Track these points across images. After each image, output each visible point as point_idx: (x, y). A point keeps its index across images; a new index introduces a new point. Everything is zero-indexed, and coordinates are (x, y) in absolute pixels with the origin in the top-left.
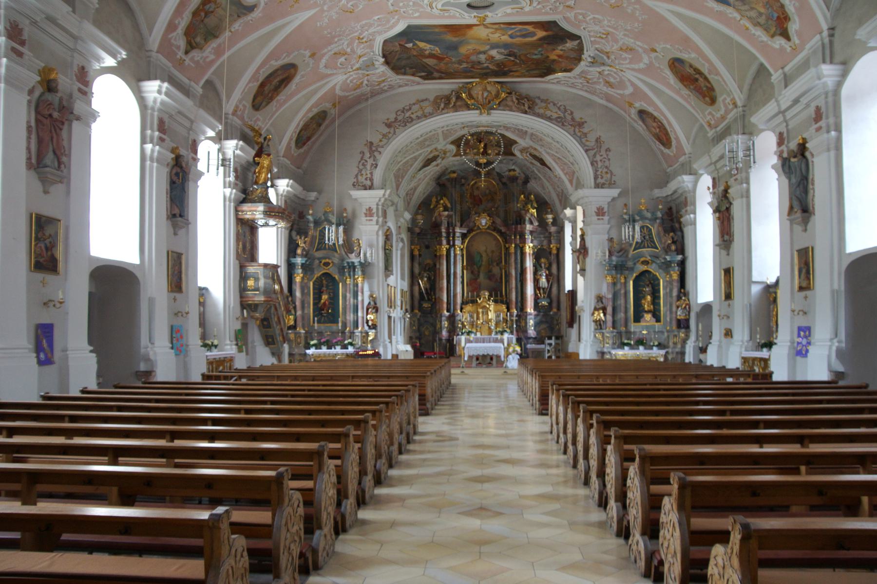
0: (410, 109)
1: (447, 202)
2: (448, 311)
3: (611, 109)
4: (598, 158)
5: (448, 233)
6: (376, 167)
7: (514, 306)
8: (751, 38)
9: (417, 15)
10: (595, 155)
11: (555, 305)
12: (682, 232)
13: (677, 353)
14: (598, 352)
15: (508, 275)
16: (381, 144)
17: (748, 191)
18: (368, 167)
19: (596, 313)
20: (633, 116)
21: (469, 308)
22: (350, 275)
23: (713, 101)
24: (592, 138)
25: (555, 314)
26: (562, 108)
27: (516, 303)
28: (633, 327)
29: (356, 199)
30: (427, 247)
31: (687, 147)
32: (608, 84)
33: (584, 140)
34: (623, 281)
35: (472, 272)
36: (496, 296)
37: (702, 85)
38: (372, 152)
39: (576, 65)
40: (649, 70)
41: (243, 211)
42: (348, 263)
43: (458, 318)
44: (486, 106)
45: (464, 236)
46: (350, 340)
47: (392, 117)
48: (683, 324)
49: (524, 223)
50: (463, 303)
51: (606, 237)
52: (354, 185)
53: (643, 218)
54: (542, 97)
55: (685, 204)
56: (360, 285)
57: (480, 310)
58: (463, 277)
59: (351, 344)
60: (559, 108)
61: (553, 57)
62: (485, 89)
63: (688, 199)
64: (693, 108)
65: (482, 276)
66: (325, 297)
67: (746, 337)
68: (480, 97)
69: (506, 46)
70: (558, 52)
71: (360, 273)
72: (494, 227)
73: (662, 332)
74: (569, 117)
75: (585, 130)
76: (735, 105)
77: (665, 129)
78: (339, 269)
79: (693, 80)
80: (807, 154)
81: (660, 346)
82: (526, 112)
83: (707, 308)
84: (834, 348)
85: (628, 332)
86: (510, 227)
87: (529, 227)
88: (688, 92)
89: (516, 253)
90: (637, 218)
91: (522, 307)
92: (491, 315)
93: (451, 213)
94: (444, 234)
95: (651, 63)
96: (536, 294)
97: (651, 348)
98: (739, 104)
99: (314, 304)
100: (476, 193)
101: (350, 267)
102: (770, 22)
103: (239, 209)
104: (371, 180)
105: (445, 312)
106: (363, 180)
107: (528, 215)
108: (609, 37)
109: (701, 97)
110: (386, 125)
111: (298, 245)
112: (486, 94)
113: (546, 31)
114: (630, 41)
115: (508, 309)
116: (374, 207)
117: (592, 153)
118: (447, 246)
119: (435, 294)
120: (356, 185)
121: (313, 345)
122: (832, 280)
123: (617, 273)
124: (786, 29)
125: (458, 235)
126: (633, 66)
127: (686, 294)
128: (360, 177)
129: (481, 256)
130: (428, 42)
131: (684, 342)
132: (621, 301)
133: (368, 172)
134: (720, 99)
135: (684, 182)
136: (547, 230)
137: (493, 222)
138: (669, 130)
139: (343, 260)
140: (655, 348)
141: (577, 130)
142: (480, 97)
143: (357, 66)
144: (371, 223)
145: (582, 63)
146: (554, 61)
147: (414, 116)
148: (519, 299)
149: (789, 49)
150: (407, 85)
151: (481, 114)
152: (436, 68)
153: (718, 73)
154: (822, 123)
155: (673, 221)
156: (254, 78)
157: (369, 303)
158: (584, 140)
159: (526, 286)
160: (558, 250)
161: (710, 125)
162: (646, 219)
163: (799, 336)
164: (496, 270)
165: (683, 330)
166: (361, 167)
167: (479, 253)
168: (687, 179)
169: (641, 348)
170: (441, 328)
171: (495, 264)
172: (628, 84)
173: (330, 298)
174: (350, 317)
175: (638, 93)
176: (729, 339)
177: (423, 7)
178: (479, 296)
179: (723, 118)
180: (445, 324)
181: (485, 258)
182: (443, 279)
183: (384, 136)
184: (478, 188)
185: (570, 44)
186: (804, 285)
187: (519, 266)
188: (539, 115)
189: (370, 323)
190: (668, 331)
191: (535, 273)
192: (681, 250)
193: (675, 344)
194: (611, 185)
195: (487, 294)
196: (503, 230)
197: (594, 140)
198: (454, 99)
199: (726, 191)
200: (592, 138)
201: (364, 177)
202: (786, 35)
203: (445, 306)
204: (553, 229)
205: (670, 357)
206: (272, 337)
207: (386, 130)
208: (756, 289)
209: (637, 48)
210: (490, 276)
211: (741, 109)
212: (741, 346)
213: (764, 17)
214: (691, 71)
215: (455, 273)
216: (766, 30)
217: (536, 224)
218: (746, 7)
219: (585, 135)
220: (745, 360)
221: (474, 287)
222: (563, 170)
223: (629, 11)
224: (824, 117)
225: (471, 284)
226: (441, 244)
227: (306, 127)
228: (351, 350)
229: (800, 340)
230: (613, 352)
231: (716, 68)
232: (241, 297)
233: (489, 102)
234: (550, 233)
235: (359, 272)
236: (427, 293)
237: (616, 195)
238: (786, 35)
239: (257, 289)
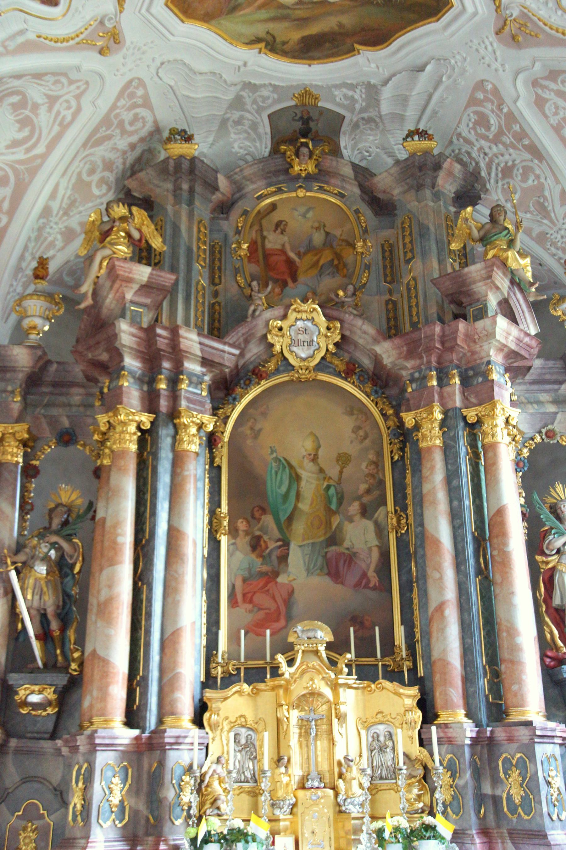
1: (149, 229)
2: (133, 718)
5: (151, 357)
7: (456, 693)
15: (413, 549)
21: (234, 704)
27: (468, 679)
30: (67, 438)
35: (256, 545)
36: (365, 647)
43: (178, 758)
45: (224, 389)
49: (482, 313)
50: (209, 682)
57: (294, 715)
58: (212, 562)
65: (297, 557)
72: (344, 358)
89: (449, 451)
91: (497, 707)
92: (349, 741)
93: (168, 278)
94: (131, 363)
100: (273, 241)
115: (428, 708)
118: (146, 419)
119: (81, 641)
125: (193, 367)
129: (296, 478)
148: (481, 660)
164: (359, 535)
171: (354, 508)
181: (310, 485)
182: (113, 561)
184: (280, 226)
187: (468, 502)
191: (535, 544)
195: (324, 634)
196: (388, 352)
203: (118, 692)
210: (335, 563)
215: (174, 536)
221: (262, 605)
225: (248, 598)
226: (112, 401)
236: (44, 636)
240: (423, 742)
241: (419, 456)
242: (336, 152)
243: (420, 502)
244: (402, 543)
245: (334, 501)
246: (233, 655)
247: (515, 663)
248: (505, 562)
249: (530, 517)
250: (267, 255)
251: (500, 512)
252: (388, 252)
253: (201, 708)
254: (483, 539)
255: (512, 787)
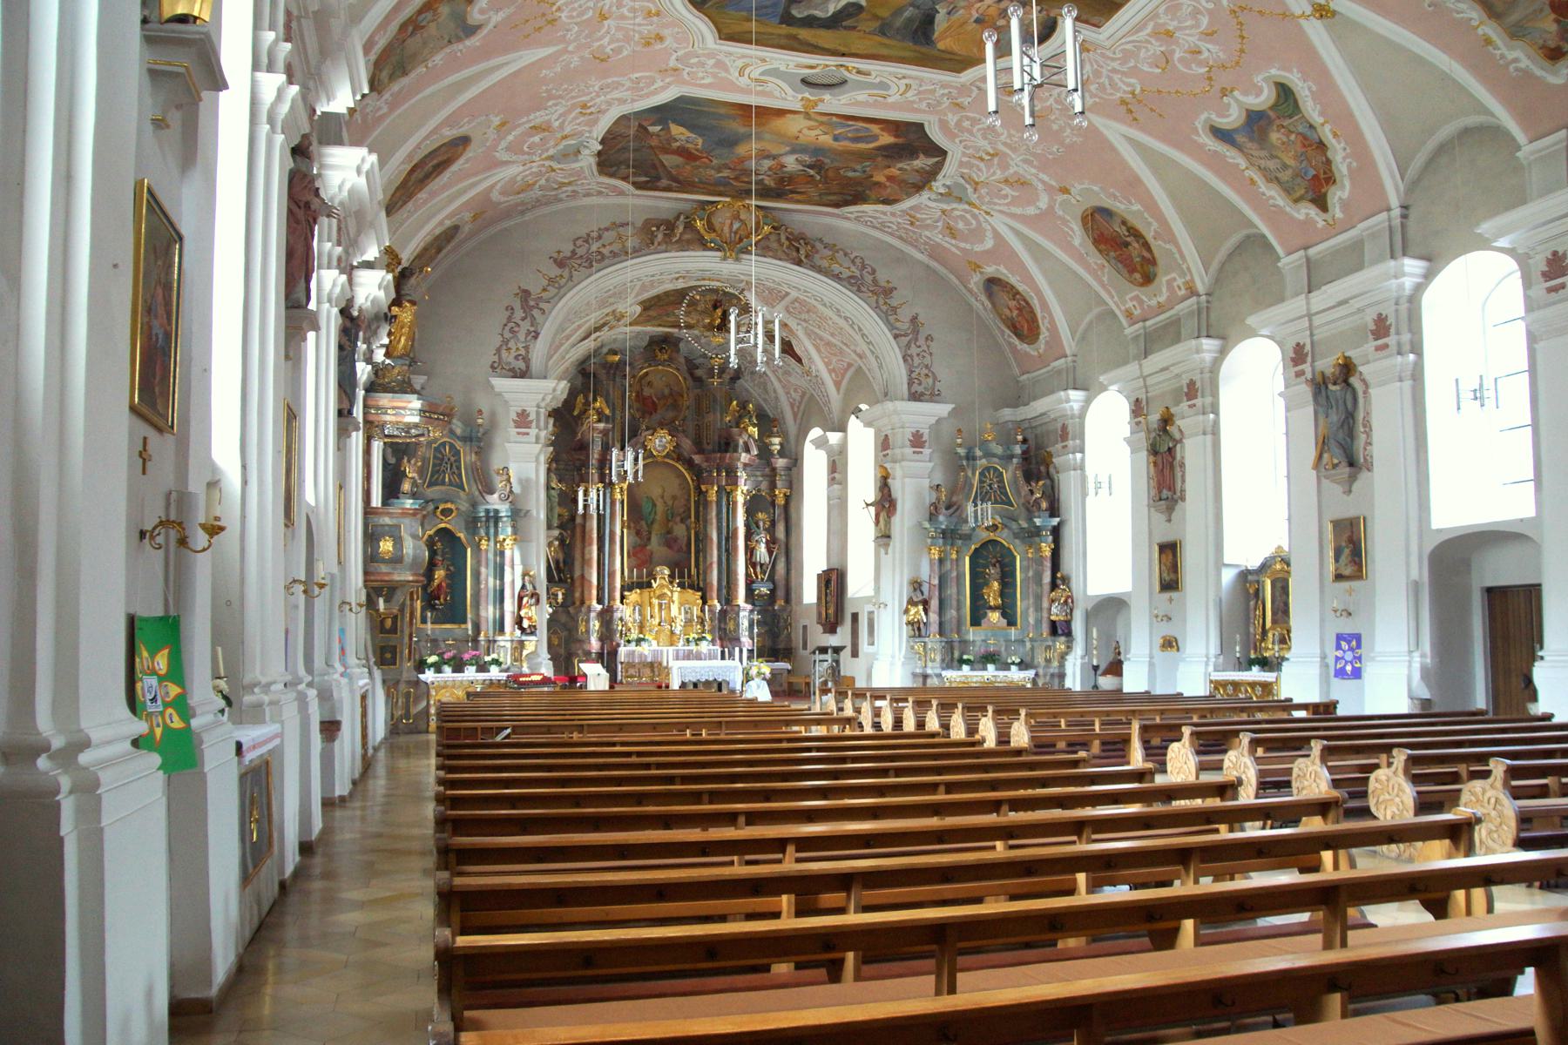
0: (600, 237)
1: (604, 406)
2: (600, 601)
3: (934, 271)
4: (914, 350)
6: (536, 337)
7: (715, 595)
8: (1258, 202)
9: (708, 81)
10: (908, 346)
11: (781, 593)
12: (1052, 481)
13: (1052, 675)
14: (914, 675)
15: (702, 540)
16: (544, 295)
17: (1216, 424)
18: (522, 336)
19: (913, 610)
20: (972, 285)
21: (633, 596)
22: (487, 534)
23: (1148, 279)
24: (905, 315)
25: (783, 609)
26: (858, 261)
27: (719, 590)
28: (972, 634)
29: (499, 394)
31: (1069, 344)
32: (951, 232)
33: (891, 318)
34: (954, 556)
35: (638, 533)
36: (681, 576)
37: (1135, 253)
38: (526, 308)
39: (909, 195)
40: (1042, 220)
41: (378, 408)
42: (487, 511)
43: (617, 615)
44: (735, 246)
46: (494, 656)
47: (567, 248)
48: (1060, 630)
49: (736, 450)
50: (623, 589)
51: (926, 483)
52: (492, 367)
53: (988, 454)
54: (826, 240)
55: (1064, 434)
56: (508, 553)
59: (496, 662)
60: (853, 262)
61: (879, 177)
62: (737, 217)
63: (1070, 428)
64: (1103, 286)
65: (654, 539)
66: (440, 574)
67: (1214, 649)
68: (726, 229)
69: (818, 151)
70: (894, 171)
71: (509, 530)
73: (1022, 642)
74: (868, 279)
75: (894, 303)
76: (1193, 292)
77: (1032, 312)
78: (467, 523)
79: (1122, 245)
80: (1353, 380)
81: (1023, 665)
82: (799, 263)
83: (1112, 607)
84: (1416, 666)
85: (964, 643)
86: (707, 454)
87: (744, 457)
88: (1101, 261)
90: (978, 453)
91: (728, 598)
92: (674, 609)
95: (1051, 208)
96: (748, 575)
97: (1006, 666)
98: (1201, 288)
99: (425, 588)
100: (647, 392)
101: (488, 520)
102: (1299, 180)
103: (370, 403)
104: (526, 360)
105: (594, 602)
106: (511, 359)
107: (745, 437)
108: (996, 160)
109: (1125, 272)
110: (555, 261)
111: (404, 474)
112: (736, 225)
113: (896, 136)
114: (1029, 172)
115: (704, 600)
116: (532, 411)
117: (905, 340)
120: (498, 368)
121: (433, 665)
122: (1408, 564)
123: (945, 544)
124: (1325, 195)
126: (1014, 210)
127: (1066, 580)
128: (504, 354)
129: (654, 505)
130: (691, 127)
131: (1063, 657)
132: (952, 591)
133: (520, 345)
134: (1163, 280)
135: (1068, 400)
136: (769, 464)
137: (678, 446)
138: (1039, 316)
139: (474, 505)
140: (1013, 668)
141: (881, 302)
142: (726, 229)
143: (551, 152)
144: (525, 438)
145: (925, 194)
146: (878, 184)
147: (605, 251)
149: (1321, 224)
150: (600, 193)
151: (725, 258)
152: (674, 172)
153: (1173, 240)
154: (1391, 340)
155: (1038, 463)
156: (410, 156)
157: (523, 587)
158: (891, 318)
159: (736, 560)
160: (787, 498)
161: (1129, 314)
162: (994, 455)
163: (1339, 647)
164: (679, 530)
165: (1063, 639)
166: (507, 335)
167: (650, 499)
168: (1076, 396)
169: (991, 667)
170: (588, 631)
172: (989, 234)
173: (447, 576)
174: (489, 612)
175: (1002, 250)
176: (1172, 653)
177: (727, 71)
178: (652, 576)
179: (1161, 308)
180: (595, 625)
181: (660, 508)
183: (551, 280)
185: (922, 162)
186: (1347, 572)
188: (819, 270)
189: (526, 624)
190: (1032, 640)
191: (748, 537)
192: (1054, 510)
193: (1048, 661)
194: (934, 396)
195: (667, 572)
197: (908, 319)
198: (681, 228)
199: (1167, 420)
200: (905, 315)
201: (513, 354)
202: (1321, 203)
203: (594, 592)
204: (780, 463)
205: (1040, 683)
206: (393, 650)
207: (555, 271)
208: (1228, 576)
209: (1035, 182)
210: (669, 541)
211: (1203, 298)
212: (1207, 664)
213: (1289, 172)
214: (1123, 231)
216: (1288, 190)
217: (755, 452)
218: (1263, 153)
219: (894, 310)
220: (1217, 685)
221: (642, 559)
222: (827, 364)
223: (1055, 127)
224: (1392, 330)
227: (425, 249)
228: (495, 673)
229: (1340, 653)
230: (944, 673)
231: (1170, 229)
232: (366, 573)
233: (741, 240)
234: (774, 469)
235: (506, 531)
237: (945, 414)
238: (1321, 203)
239: (397, 560)
240: (703, 610)
241: (706, 504)
242: (678, 351)
243: (706, 521)
244: (697, 534)
245: (669, 517)
246: (631, 576)
247: (736, 585)
248: (736, 548)
249: (747, 525)
250: (645, 399)
251: (736, 530)
252: (698, 400)
253: (623, 597)
254: (729, 538)
255: (731, 626)
